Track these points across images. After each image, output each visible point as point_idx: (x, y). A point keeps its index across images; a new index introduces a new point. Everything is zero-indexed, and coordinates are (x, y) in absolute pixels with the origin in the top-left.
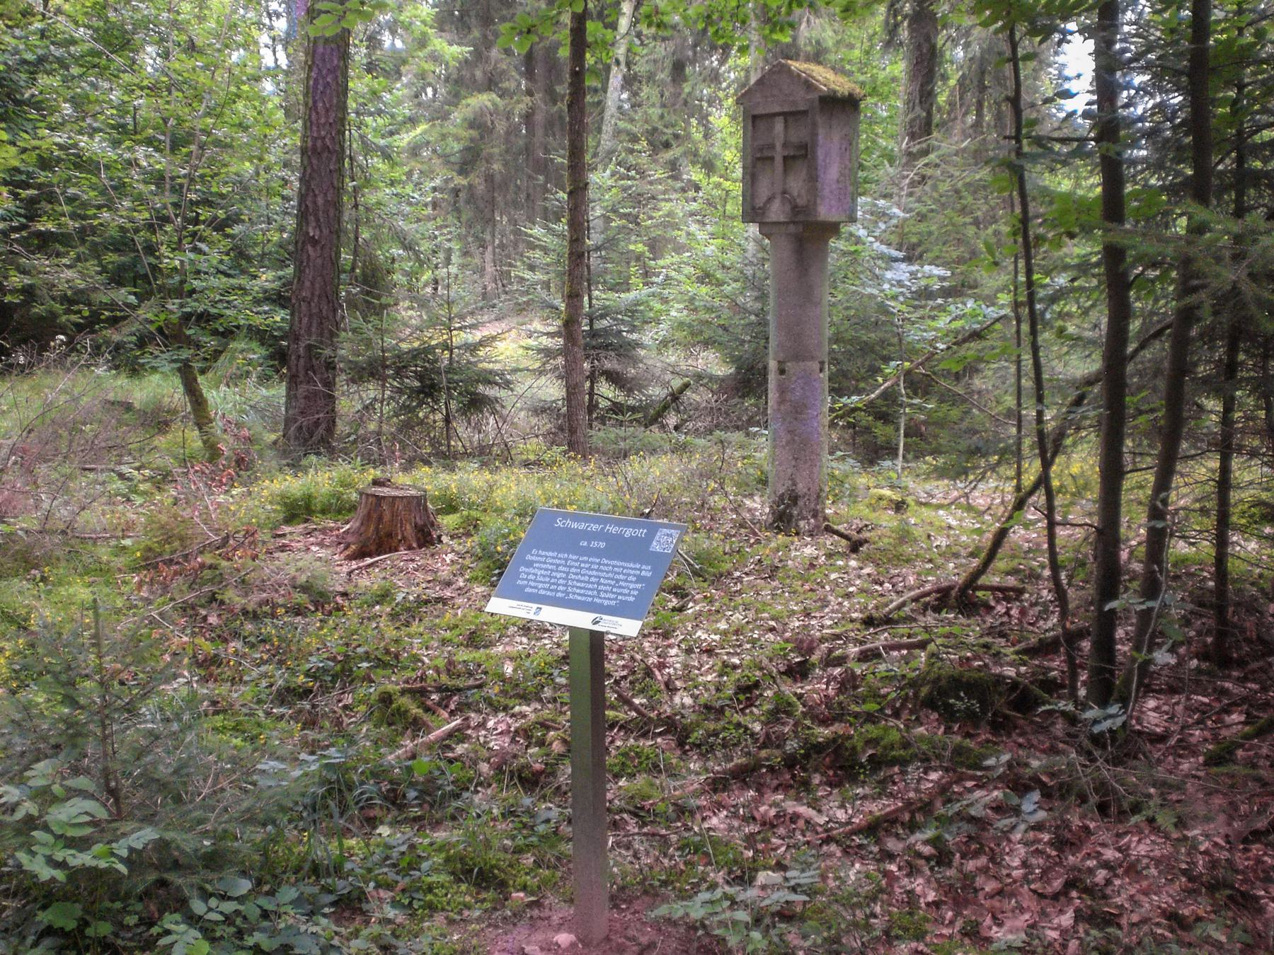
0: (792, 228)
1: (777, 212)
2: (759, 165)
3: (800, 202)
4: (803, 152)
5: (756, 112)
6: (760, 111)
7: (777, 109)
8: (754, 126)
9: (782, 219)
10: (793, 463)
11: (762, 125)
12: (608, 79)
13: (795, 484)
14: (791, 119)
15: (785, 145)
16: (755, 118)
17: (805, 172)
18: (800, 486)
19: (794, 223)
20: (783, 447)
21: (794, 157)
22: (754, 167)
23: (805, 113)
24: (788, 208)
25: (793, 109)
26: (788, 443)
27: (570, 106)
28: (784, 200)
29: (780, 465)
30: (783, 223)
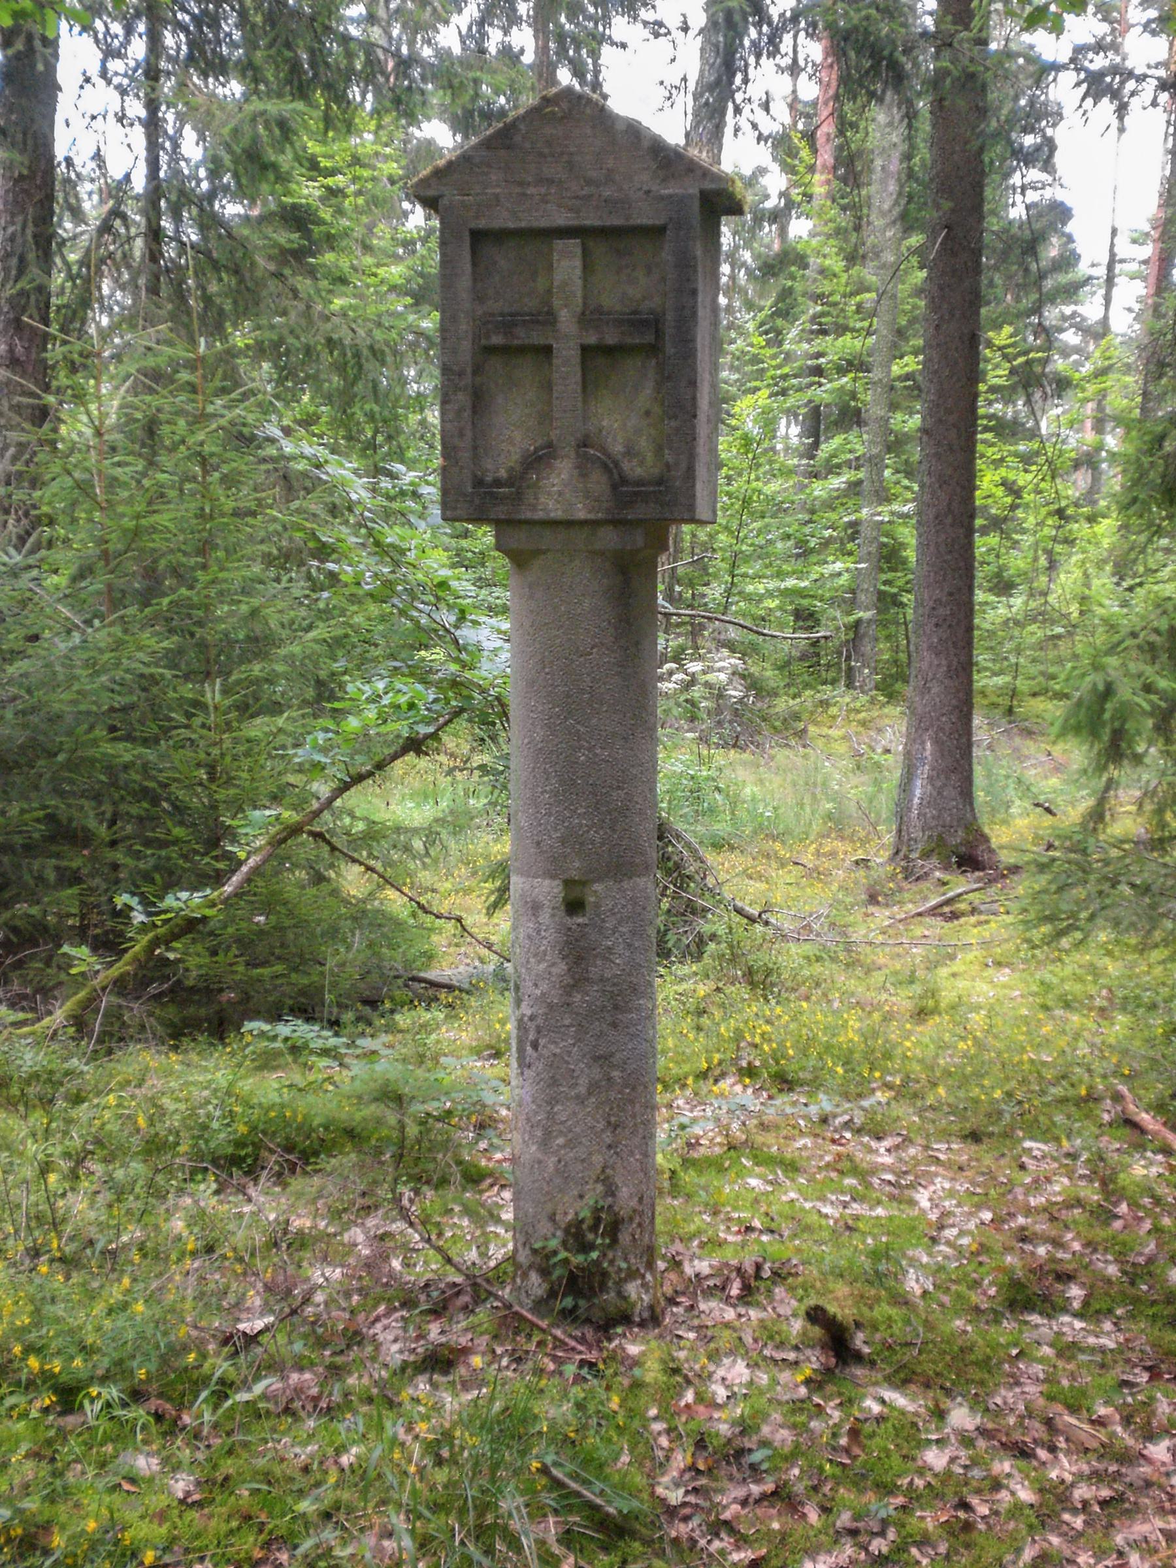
0: (608, 538)
1: (560, 492)
2: (495, 364)
3: (633, 469)
4: (649, 338)
5: (482, 224)
6: (501, 219)
7: (562, 219)
8: (474, 252)
9: (581, 513)
10: (608, 1138)
11: (502, 259)
12: (971, 770)
13: (611, 1191)
14: (600, 249)
15: (590, 317)
16: (478, 236)
17: (648, 389)
18: (624, 1192)
19: (616, 523)
20: (581, 1100)
21: (609, 351)
22: (477, 370)
23: (656, 232)
24: (598, 482)
25: (617, 221)
26: (593, 1087)
27: (879, 1139)
28: (583, 466)
29: (570, 1144)
30: (583, 523)
